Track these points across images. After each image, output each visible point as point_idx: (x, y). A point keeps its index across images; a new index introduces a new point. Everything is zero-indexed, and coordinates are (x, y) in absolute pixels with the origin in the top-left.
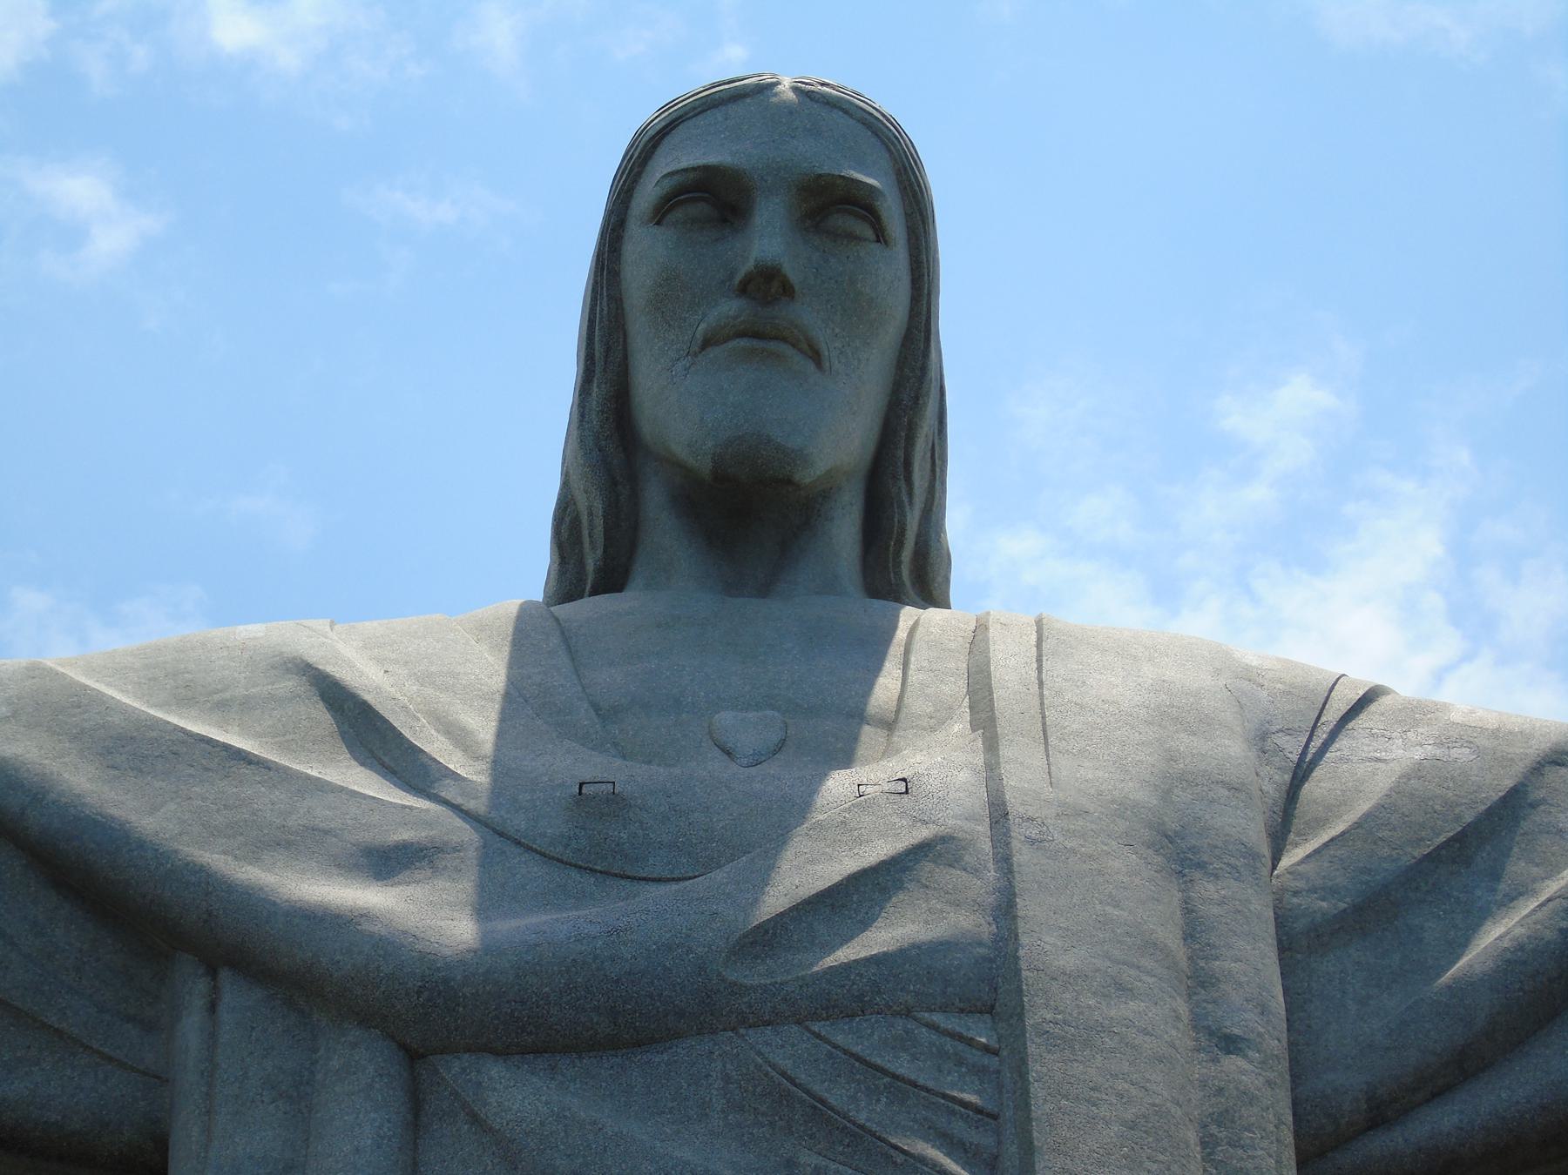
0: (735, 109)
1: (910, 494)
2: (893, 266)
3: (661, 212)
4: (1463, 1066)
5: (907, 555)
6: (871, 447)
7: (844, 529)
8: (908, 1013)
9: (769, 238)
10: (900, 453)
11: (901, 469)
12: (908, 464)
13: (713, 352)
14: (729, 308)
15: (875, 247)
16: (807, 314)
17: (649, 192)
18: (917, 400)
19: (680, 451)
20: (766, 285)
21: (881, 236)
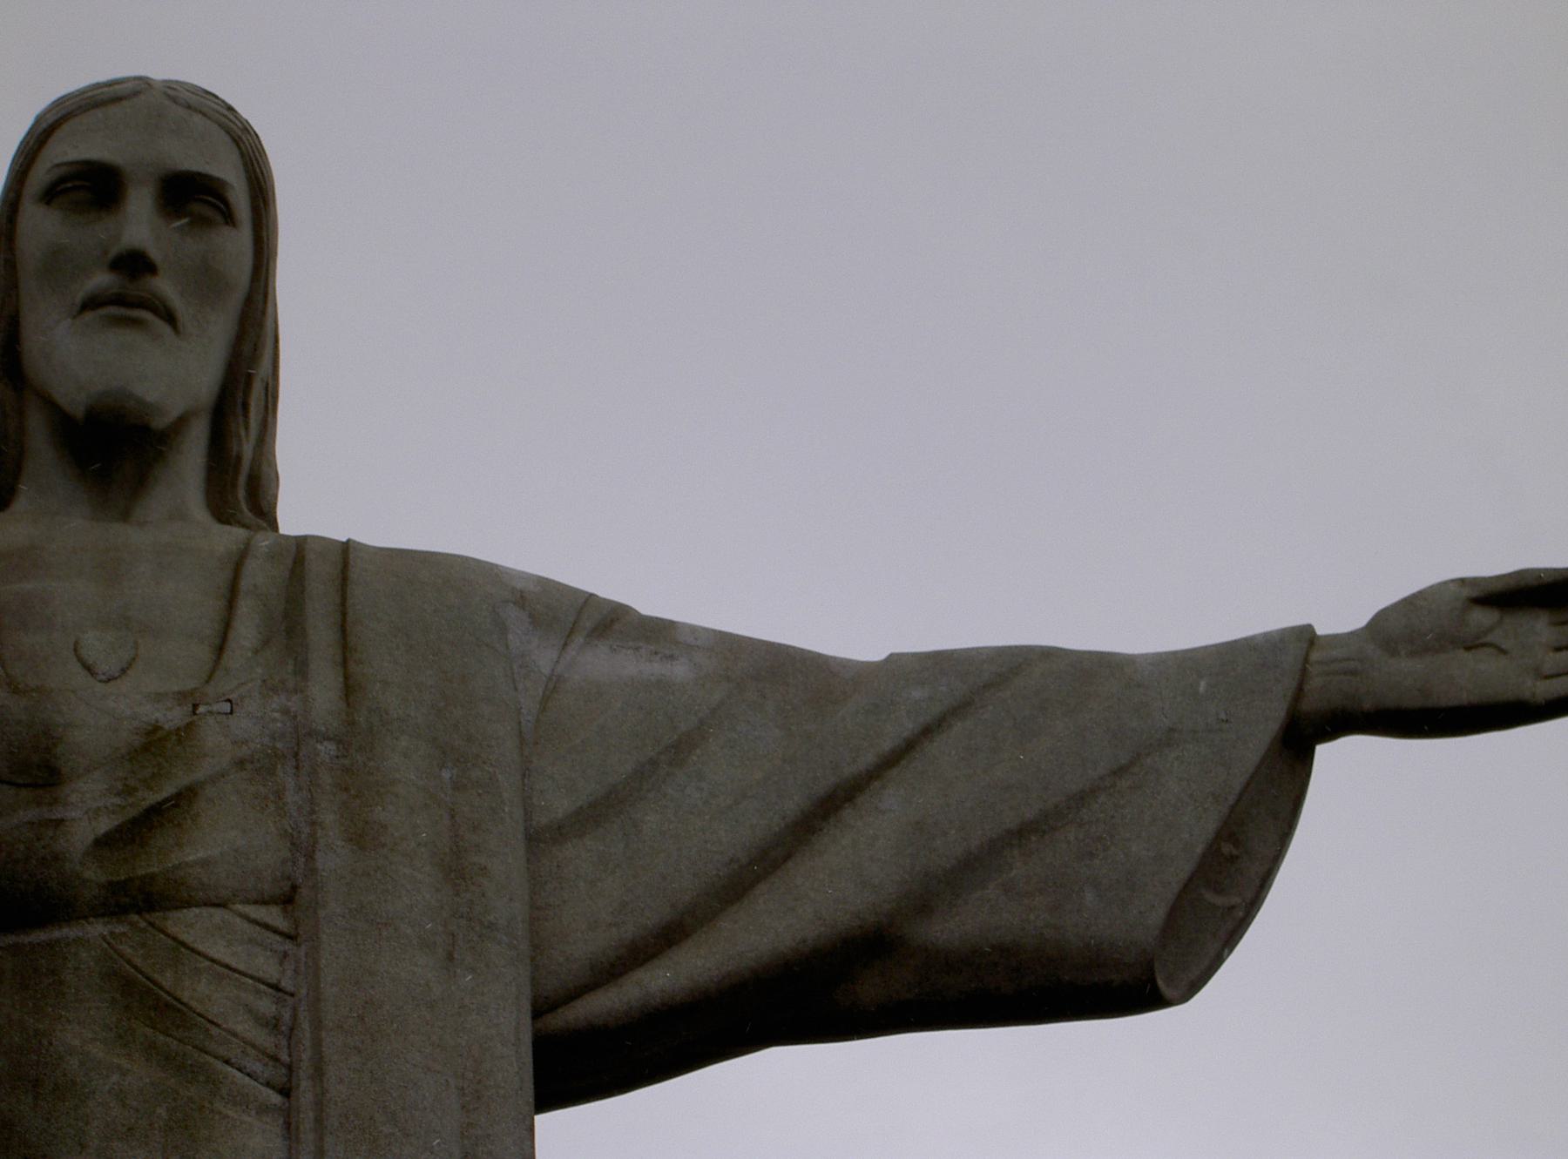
0: (113, 110)
1: (247, 428)
2: (239, 240)
3: (50, 195)
4: (669, 936)
5: (242, 480)
6: (216, 389)
7: (190, 460)
8: (222, 905)
9: (139, 223)
10: (240, 401)
11: (239, 406)
12: (245, 406)
13: (89, 316)
14: (101, 280)
15: (226, 231)
16: (165, 286)
17: (41, 175)
18: (256, 350)
19: (62, 401)
20: (134, 264)
21: (229, 218)
